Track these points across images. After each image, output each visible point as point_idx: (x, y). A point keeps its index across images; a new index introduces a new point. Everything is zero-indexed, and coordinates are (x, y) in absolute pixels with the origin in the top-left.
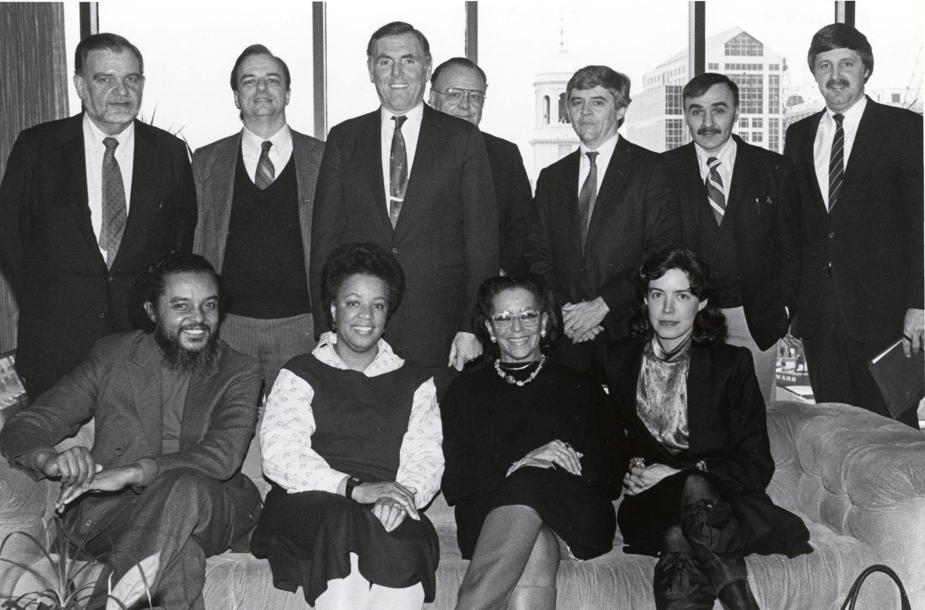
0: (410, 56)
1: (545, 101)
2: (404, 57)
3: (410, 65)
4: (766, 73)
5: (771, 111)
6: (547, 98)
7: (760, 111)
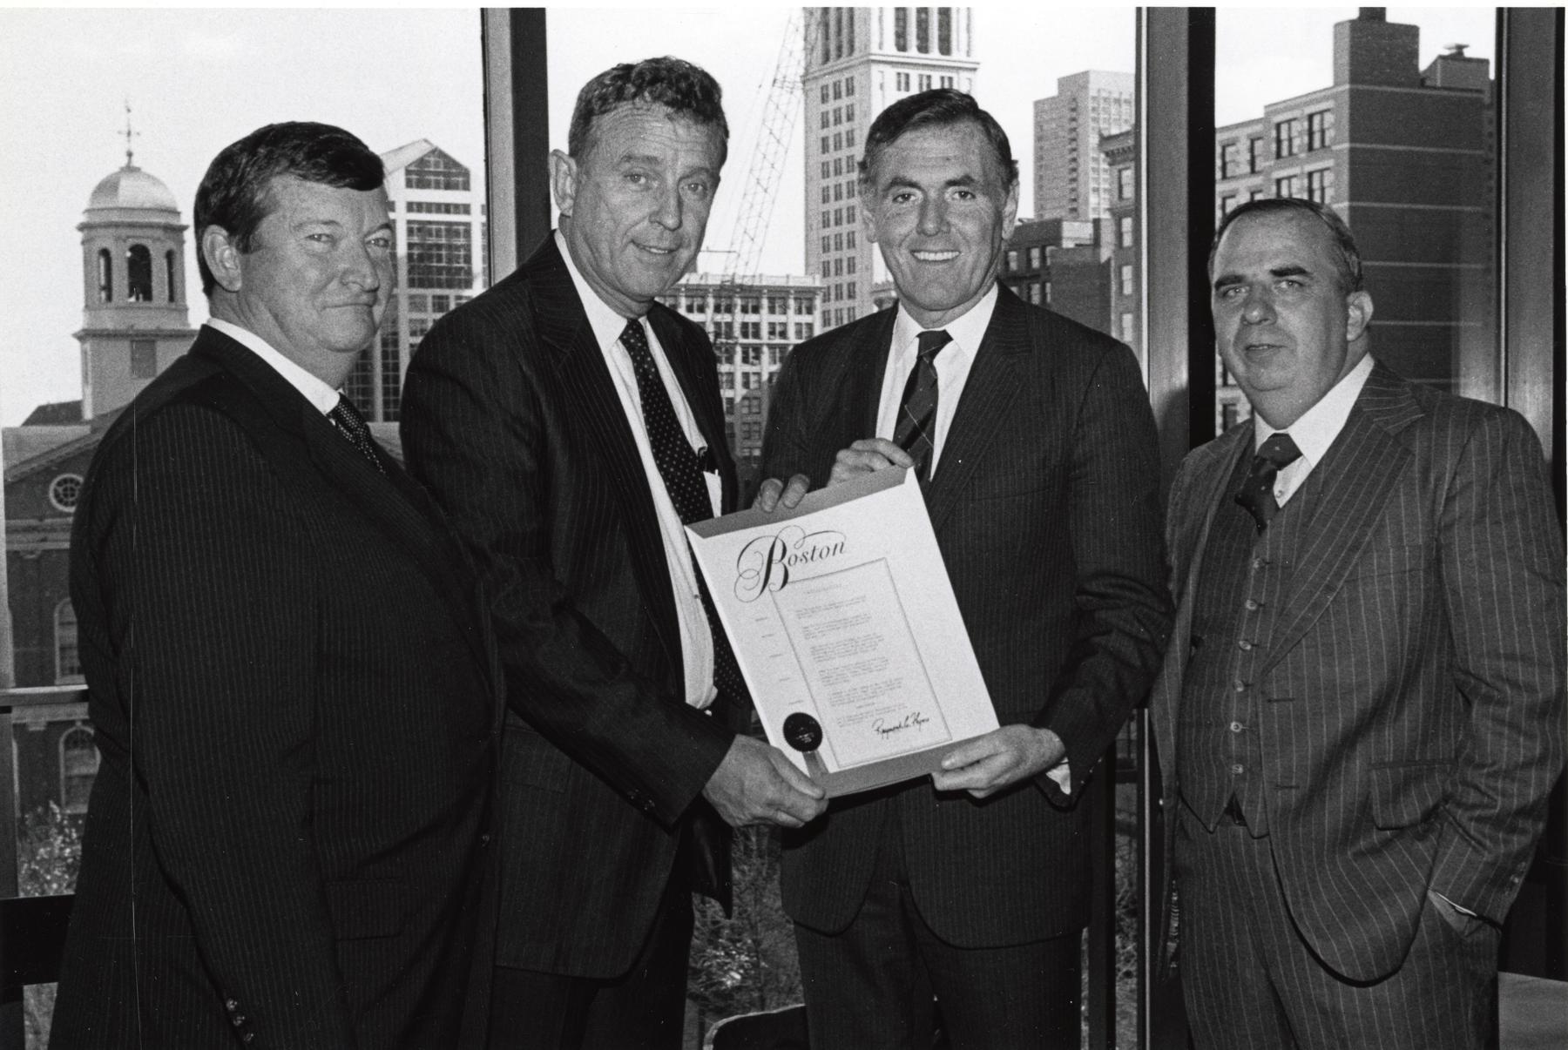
0: (966, 180)
1: (102, 261)
2: (951, 183)
3: (967, 205)
6: (105, 253)
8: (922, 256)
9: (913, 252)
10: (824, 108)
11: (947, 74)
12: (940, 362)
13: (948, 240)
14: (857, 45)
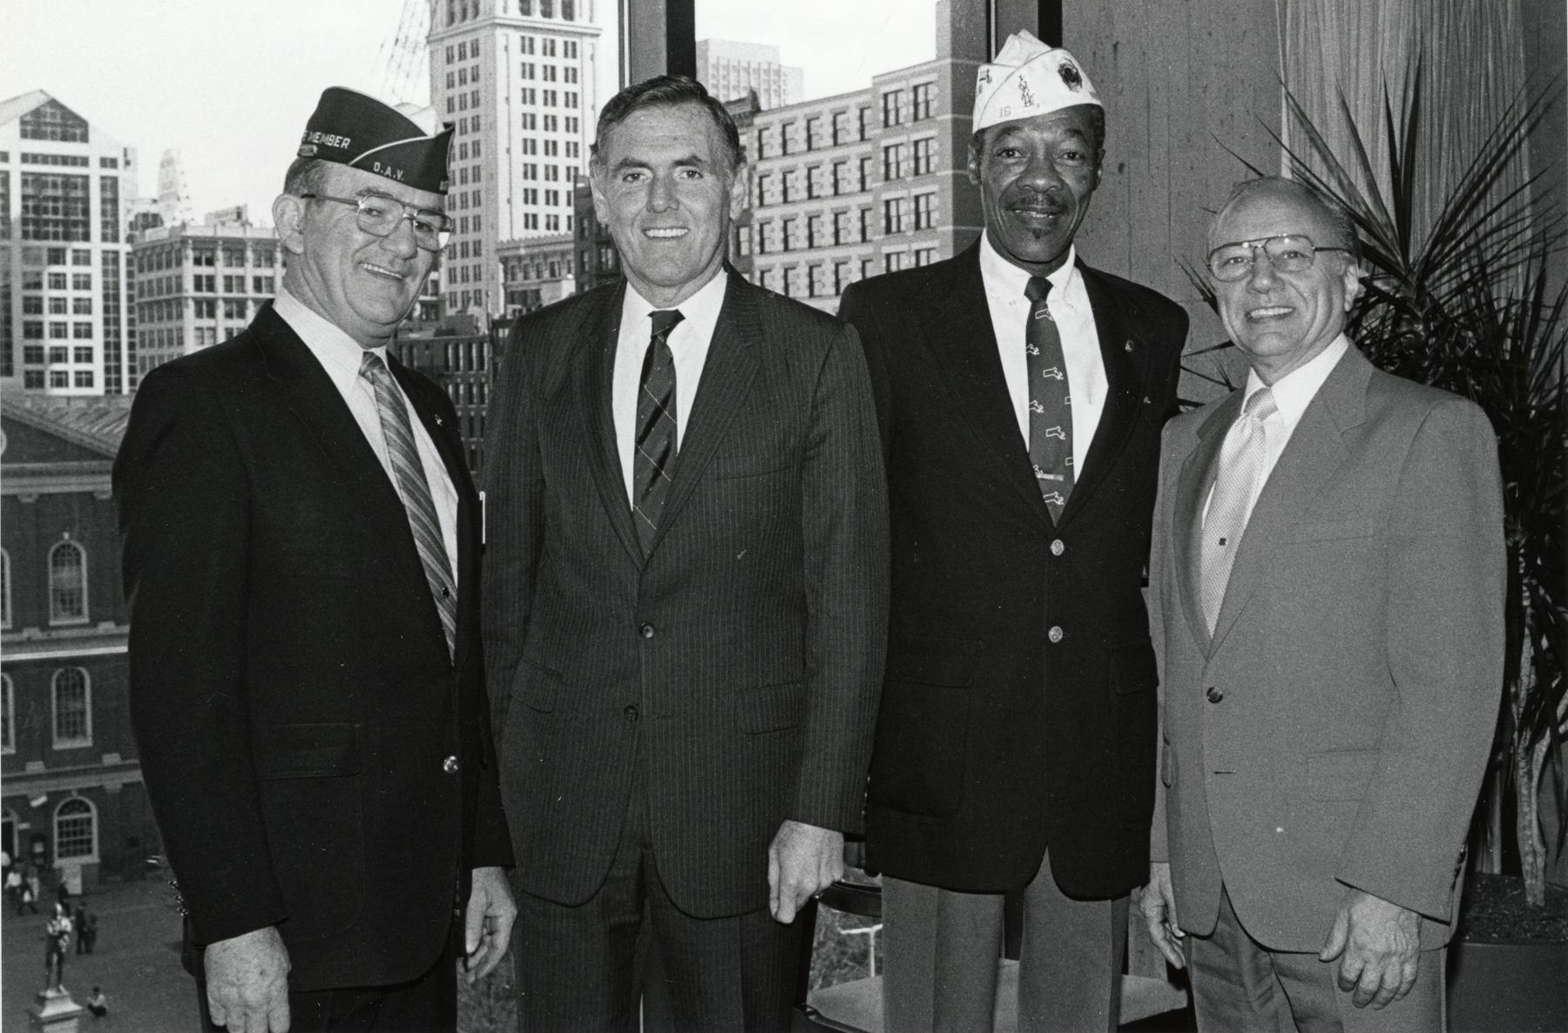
2: (680, 163)
4: (95, 172)
5: (104, 238)
7: (86, 237)
8: (651, 233)
9: (644, 231)
10: (449, 68)
11: (570, 39)
12: (674, 341)
13: (677, 219)
14: (481, 7)
